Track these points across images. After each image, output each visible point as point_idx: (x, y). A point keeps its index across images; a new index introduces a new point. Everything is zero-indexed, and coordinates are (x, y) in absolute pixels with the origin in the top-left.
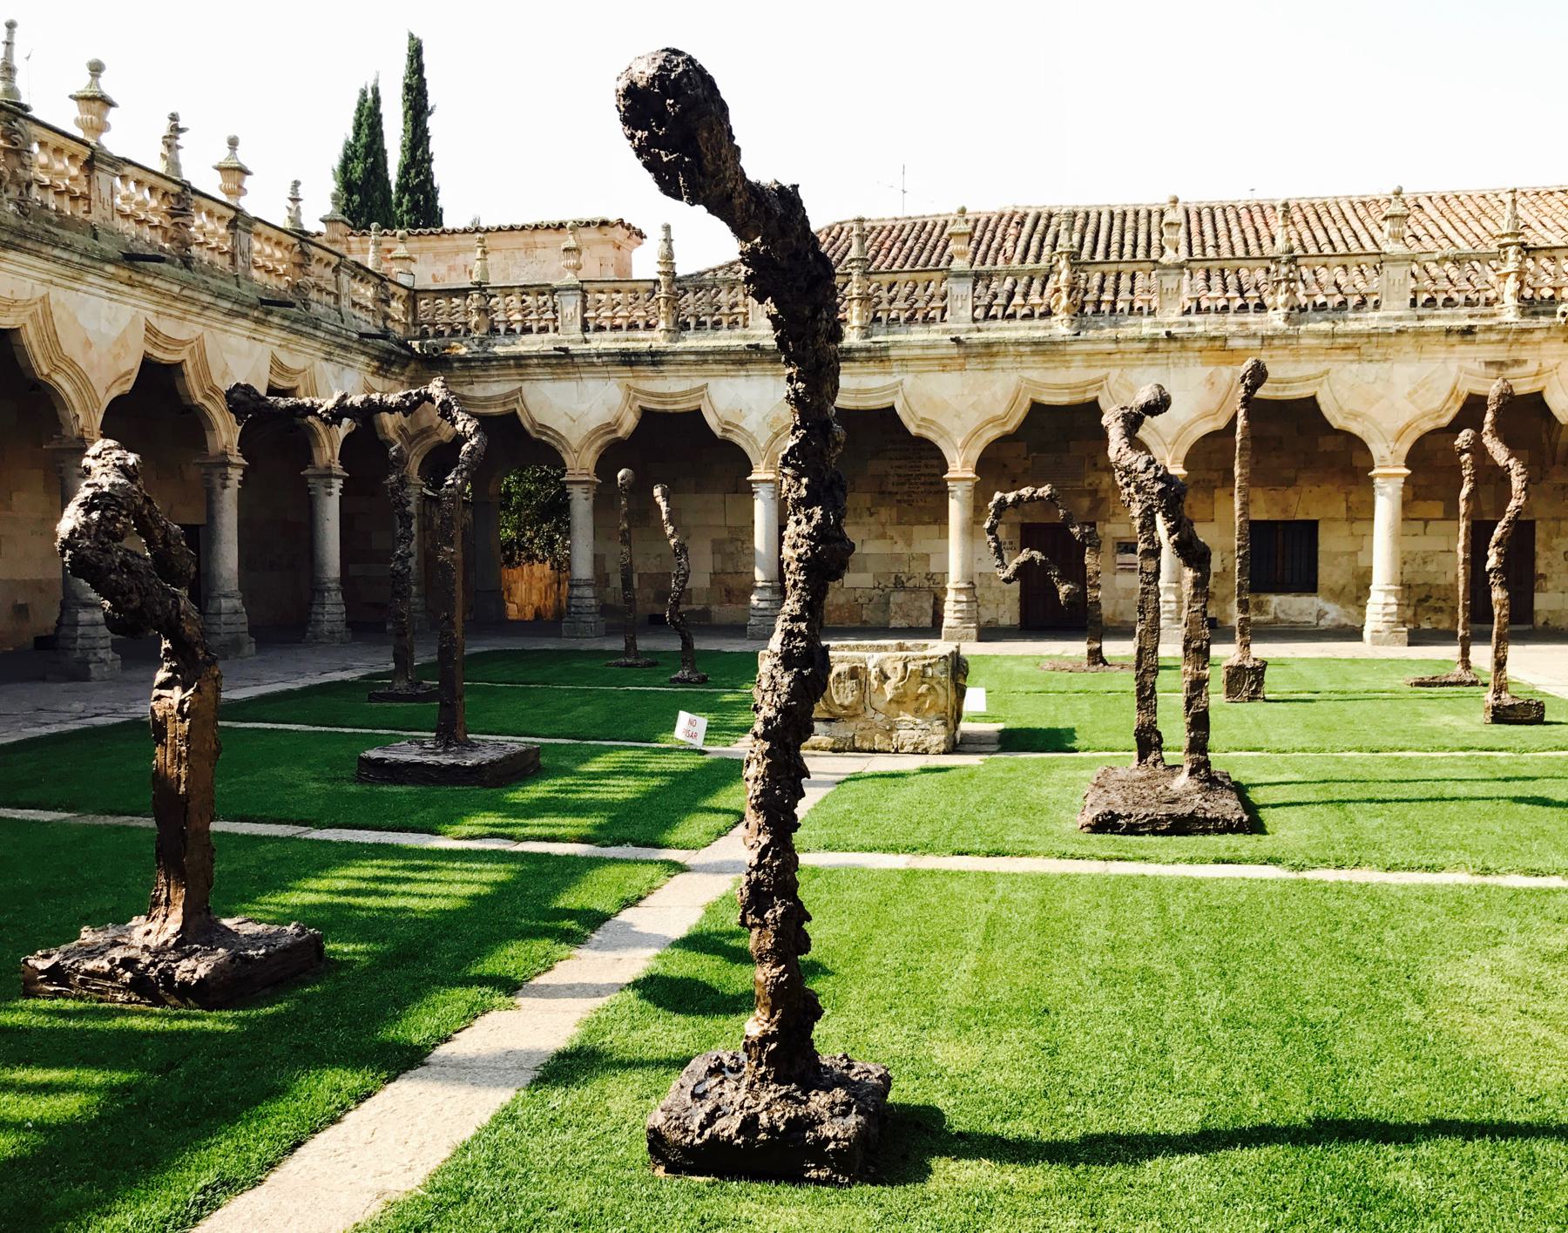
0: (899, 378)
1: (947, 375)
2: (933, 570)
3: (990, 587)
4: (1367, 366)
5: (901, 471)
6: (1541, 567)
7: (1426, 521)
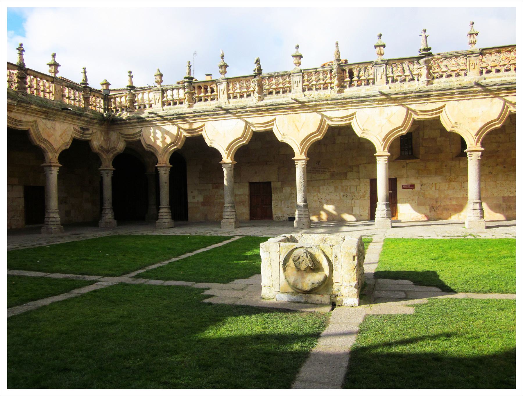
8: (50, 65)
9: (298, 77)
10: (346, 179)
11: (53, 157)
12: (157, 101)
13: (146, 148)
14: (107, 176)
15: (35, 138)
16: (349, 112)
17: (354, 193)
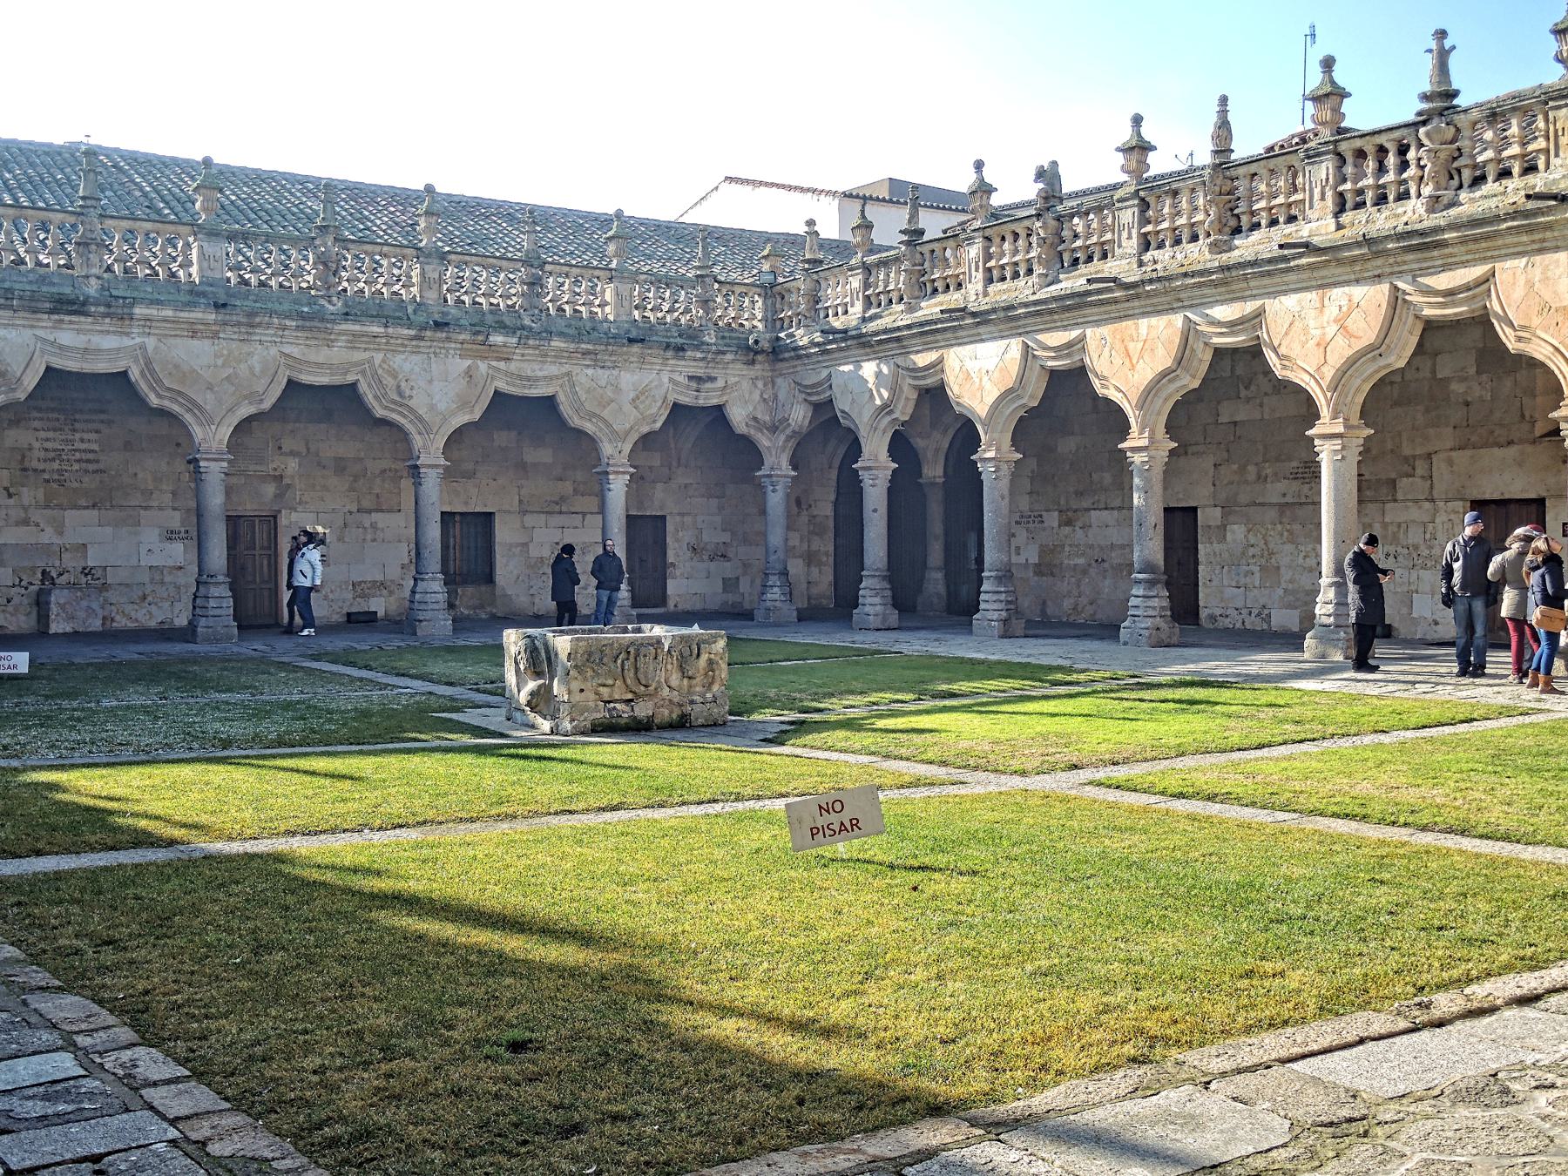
0: (138, 340)
2: (90, 564)
3: (162, 583)
4: (600, 371)
5: (49, 445)
6: (671, 558)
7: (584, 514)
9: (1129, 212)
10: (1395, 501)
11: (616, 452)
16: (1250, 307)
17: (1416, 547)
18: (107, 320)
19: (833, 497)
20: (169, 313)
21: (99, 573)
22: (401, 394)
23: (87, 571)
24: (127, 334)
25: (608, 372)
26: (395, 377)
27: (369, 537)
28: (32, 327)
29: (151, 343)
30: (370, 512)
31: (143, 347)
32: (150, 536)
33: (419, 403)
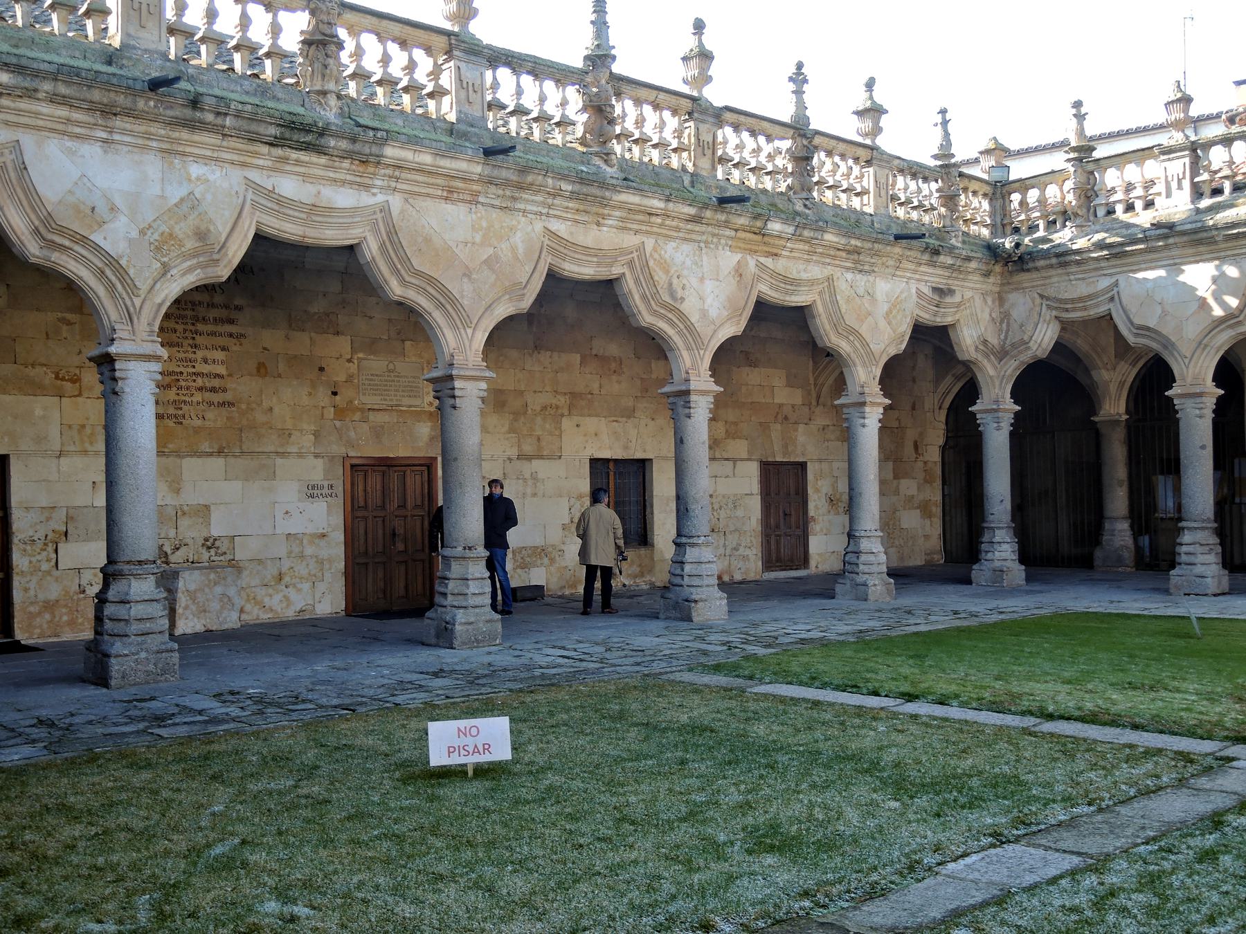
0: (380, 198)
1: (449, 207)
2: (215, 533)
3: (302, 556)
4: (859, 276)
6: (811, 513)
7: (735, 460)
8: (860, 113)
11: (865, 377)
12: (1174, 185)
13: (1131, 339)
14: (998, 429)
15: (827, 327)
18: (346, 164)
19: (941, 441)
20: (426, 158)
21: (224, 546)
22: (672, 294)
23: (210, 544)
24: (367, 187)
25: (865, 278)
26: (667, 272)
27: (529, 491)
28: (244, 165)
29: (396, 202)
30: (529, 458)
31: (385, 209)
32: (288, 493)
33: (690, 307)
